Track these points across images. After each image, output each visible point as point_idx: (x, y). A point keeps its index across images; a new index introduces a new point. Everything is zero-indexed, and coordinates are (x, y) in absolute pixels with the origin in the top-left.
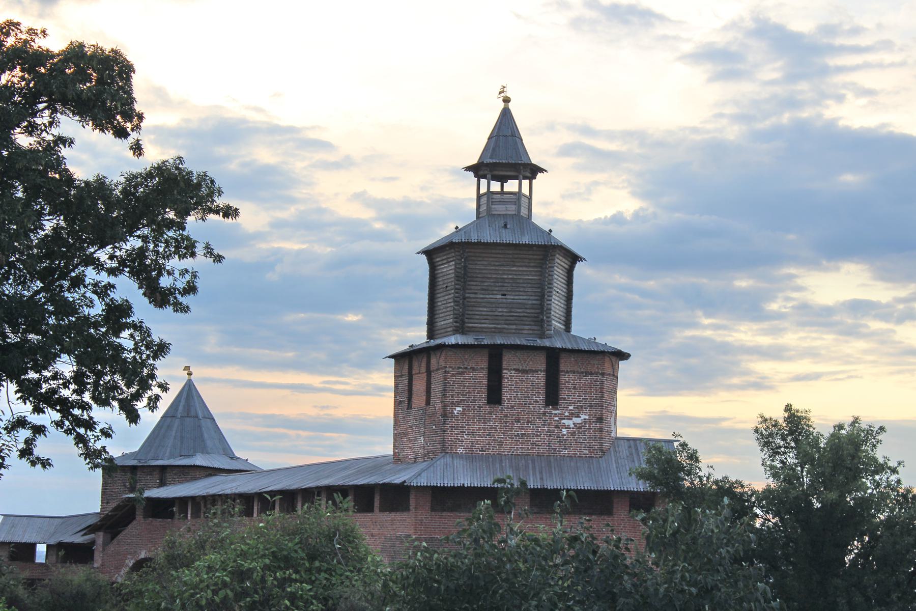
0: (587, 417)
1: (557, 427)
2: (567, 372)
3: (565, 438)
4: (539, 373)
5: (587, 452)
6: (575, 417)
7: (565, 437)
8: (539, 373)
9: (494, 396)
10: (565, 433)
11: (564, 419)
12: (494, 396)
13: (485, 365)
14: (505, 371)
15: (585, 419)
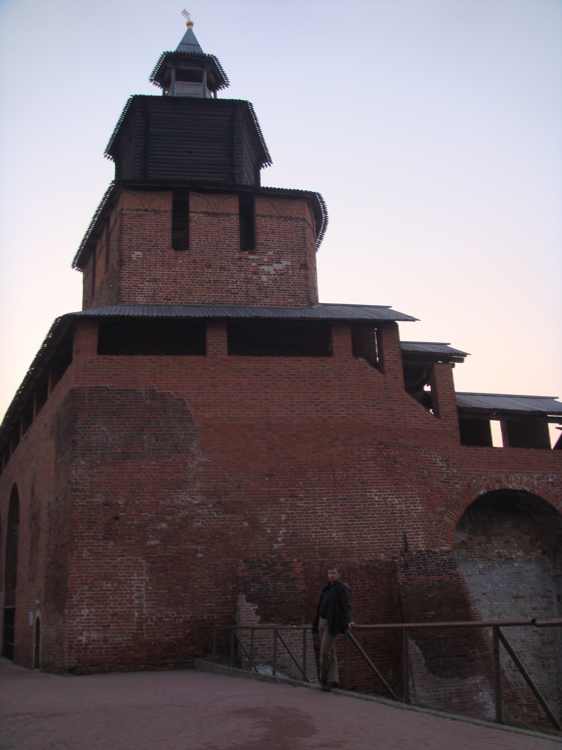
0: (289, 263)
1: (255, 273)
2: (264, 216)
4: (232, 216)
5: (292, 300)
6: (276, 263)
10: (265, 280)
11: (264, 265)
15: (287, 265)
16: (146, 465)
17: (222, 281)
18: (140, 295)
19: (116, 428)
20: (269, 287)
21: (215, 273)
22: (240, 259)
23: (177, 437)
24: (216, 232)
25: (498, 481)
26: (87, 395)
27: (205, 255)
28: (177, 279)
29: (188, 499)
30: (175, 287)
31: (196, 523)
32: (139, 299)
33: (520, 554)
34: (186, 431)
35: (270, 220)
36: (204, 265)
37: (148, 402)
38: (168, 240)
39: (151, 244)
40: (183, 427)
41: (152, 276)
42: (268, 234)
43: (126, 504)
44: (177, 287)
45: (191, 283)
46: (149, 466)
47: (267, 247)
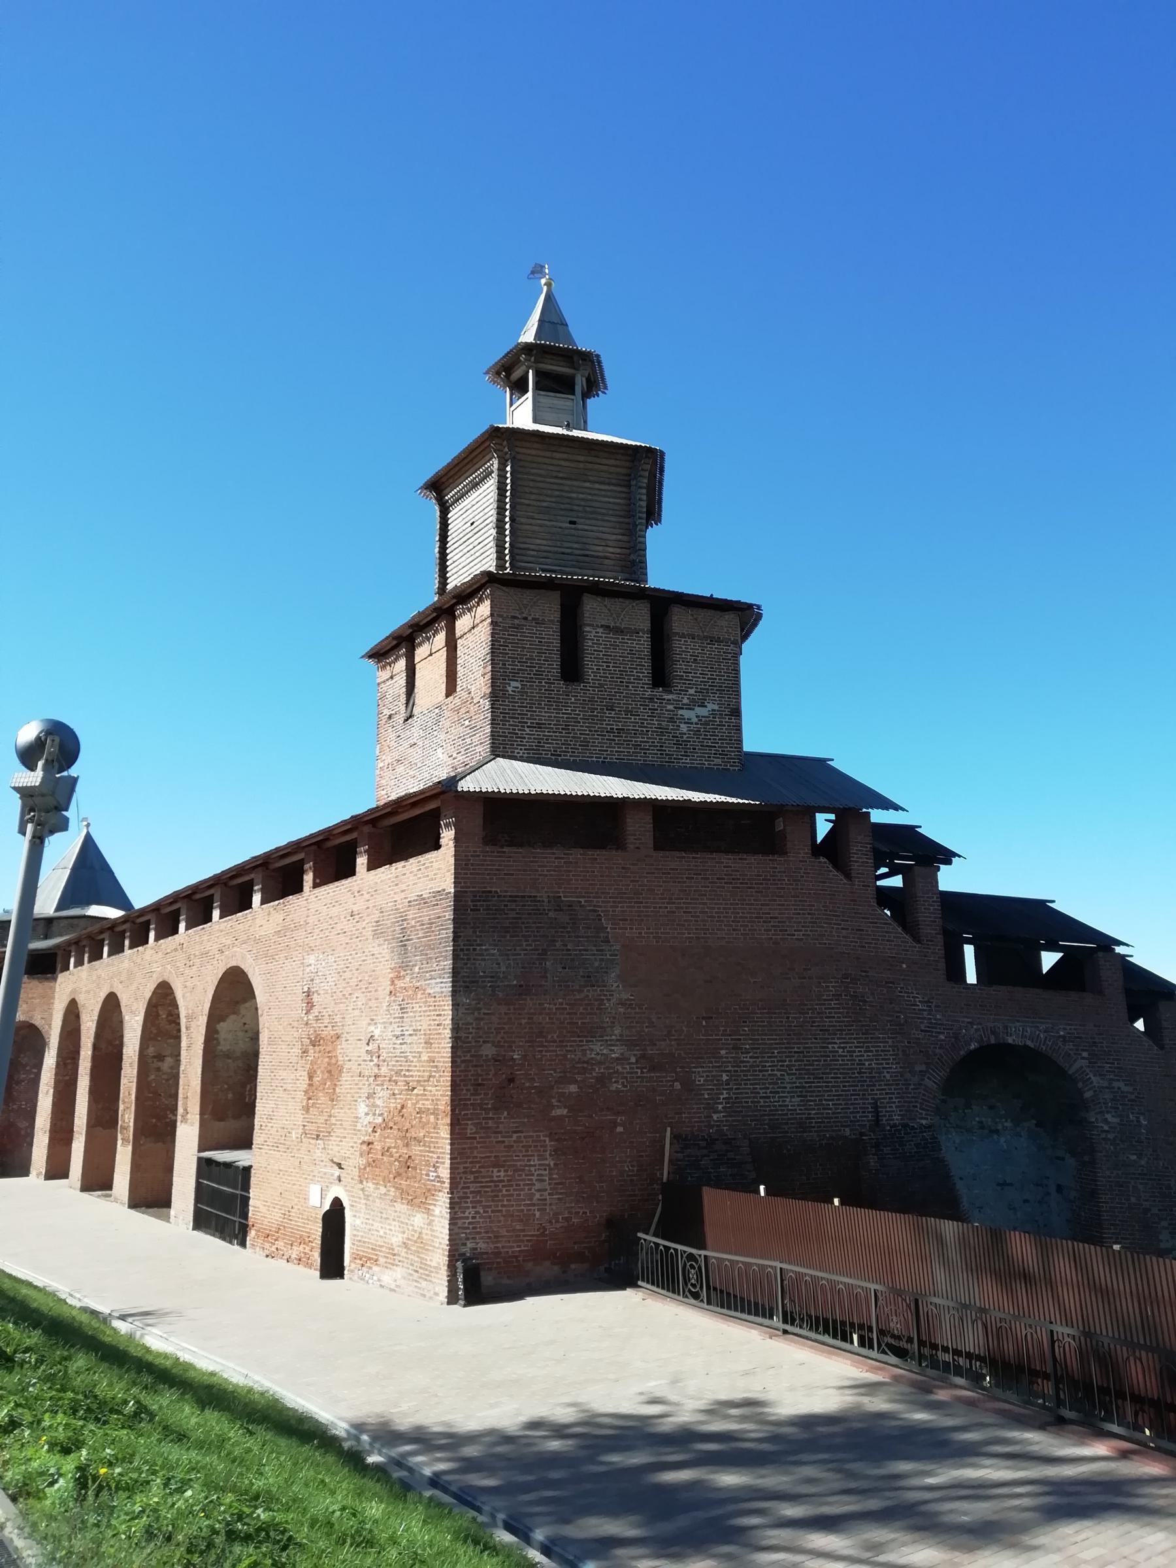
0: (716, 707)
1: (671, 720)
2: (683, 636)
3: (684, 739)
4: (641, 634)
5: (719, 761)
6: (699, 706)
7: (685, 736)
8: (641, 634)
9: (572, 670)
10: (685, 730)
11: (683, 708)
12: (572, 670)
13: (556, 616)
14: (587, 629)
16: (550, 1004)
17: (629, 730)
18: (519, 747)
19: (511, 950)
20: (690, 741)
21: (619, 718)
22: (651, 700)
23: (590, 964)
24: (620, 656)
25: (993, 1032)
26: (470, 903)
27: (606, 691)
28: (569, 725)
29: (605, 1052)
30: (566, 737)
31: (615, 1085)
32: (519, 753)
33: (1008, 1124)
34: (602, 955)
35: (691, 642)
36: (605, 706)
37: (551, 914)
38: (555, 666)
39: (533, 671)
40: (597, 950)
41: (535, 719)
42: (689, 662)
43: (524, 1057)
44: (569, 737)
45: (588, 732)
46: (555, 1004)
47: (688, 682)
